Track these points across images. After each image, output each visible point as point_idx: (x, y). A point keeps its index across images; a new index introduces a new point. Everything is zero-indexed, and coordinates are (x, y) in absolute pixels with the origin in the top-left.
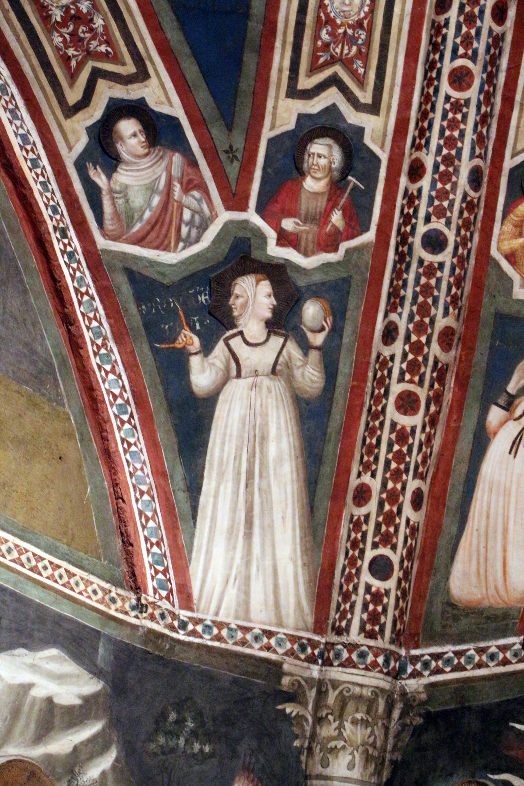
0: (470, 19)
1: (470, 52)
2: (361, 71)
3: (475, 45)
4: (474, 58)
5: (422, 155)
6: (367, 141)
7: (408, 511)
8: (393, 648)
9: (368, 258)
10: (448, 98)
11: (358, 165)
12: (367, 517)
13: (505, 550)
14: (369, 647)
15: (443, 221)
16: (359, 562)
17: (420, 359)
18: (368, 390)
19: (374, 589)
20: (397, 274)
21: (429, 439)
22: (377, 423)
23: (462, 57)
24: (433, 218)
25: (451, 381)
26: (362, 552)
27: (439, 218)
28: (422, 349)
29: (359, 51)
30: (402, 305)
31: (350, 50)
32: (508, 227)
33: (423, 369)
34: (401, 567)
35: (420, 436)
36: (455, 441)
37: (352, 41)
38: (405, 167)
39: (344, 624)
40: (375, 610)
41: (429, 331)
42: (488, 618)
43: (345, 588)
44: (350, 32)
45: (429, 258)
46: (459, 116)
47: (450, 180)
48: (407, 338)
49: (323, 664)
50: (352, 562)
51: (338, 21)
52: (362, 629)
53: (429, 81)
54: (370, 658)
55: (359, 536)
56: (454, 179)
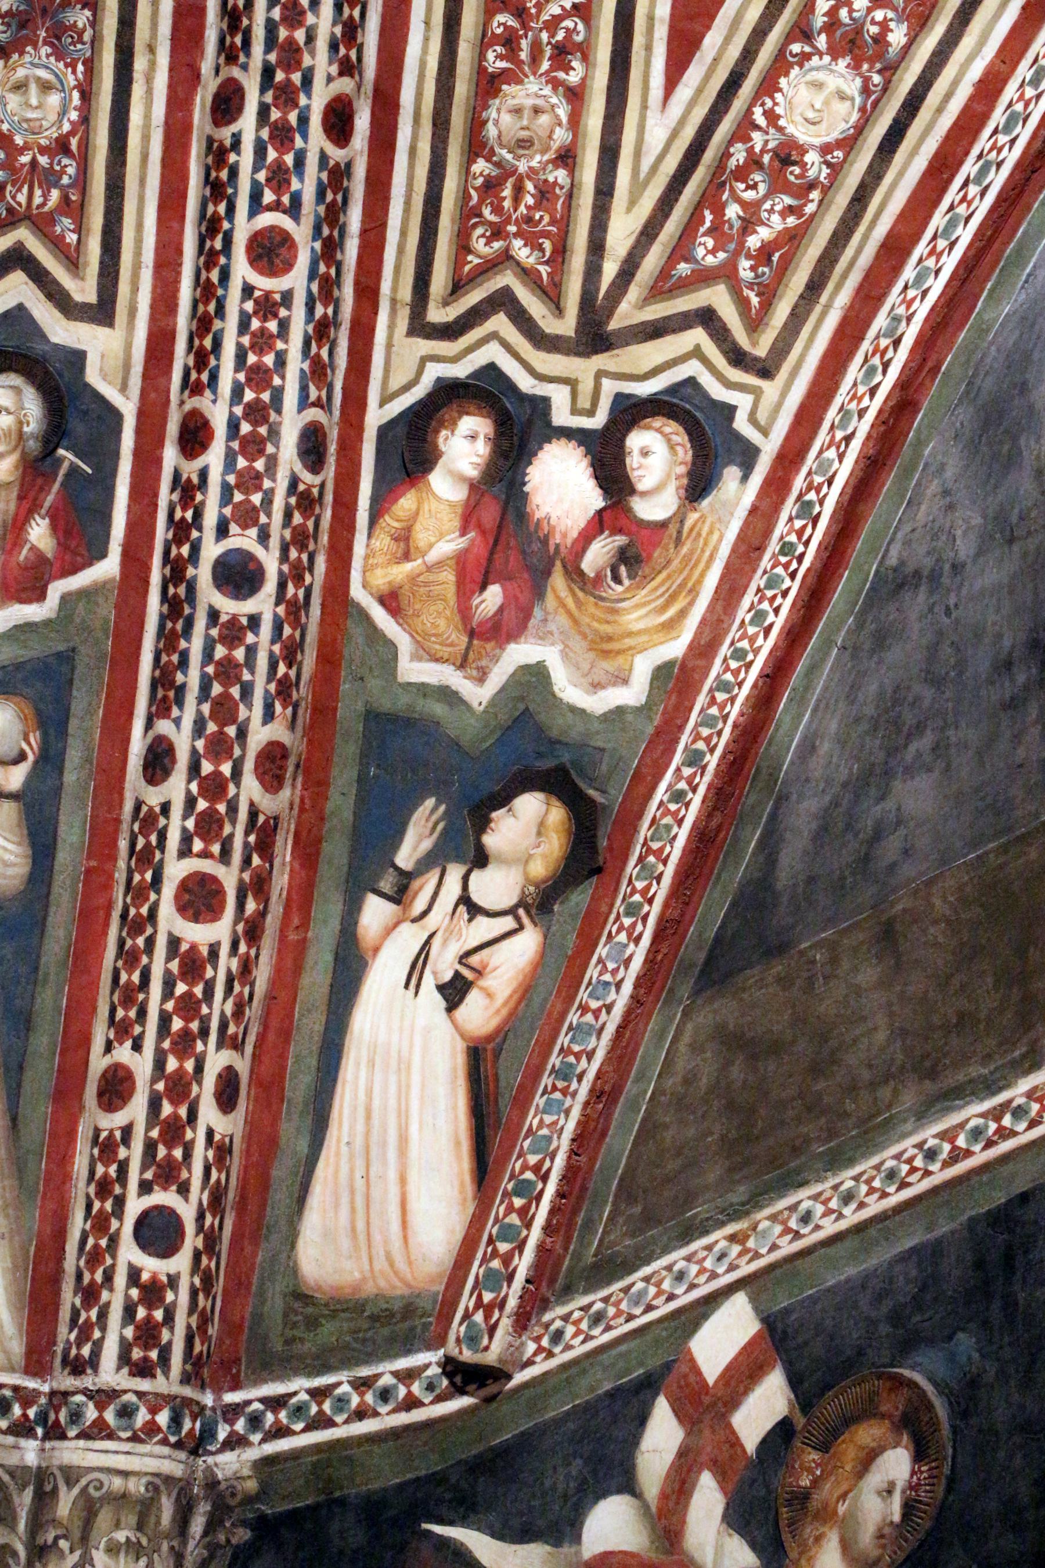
0: (282, 135)
1: (286, 199)
2: (72, 238)
3: (295, 185)
4: (294, 210)
5: (203, 403)
6: (93, 376)
7: (209, 1114)
8: (188, 1392)
9: (107, 611)
10: (248, 290)
11: (77, 426)
12: (127, 1131)
13: (403, 1180)
14: (140, 1394)
15: (253, 532)
16: (115, 1224)
17: (222, 808)
18: (120, 876)
19: (145, 1276)
20: (168, 640)
21: (247, 967)
22: (140, 941)
23: (269, 208)
24: (234, 528)
25: (284, 849)
26: (120, 1202)
27: (245, 527)
28: (224, 789)
29: (65, 199)
30: (180, 702)
31: (46, 196)
32: (382, 541)
33: (227, 830)
34: (200, 1228)
35: (227, 963)
36: (298, 969)
37: (50, 179)
38: (173, 428)
39: (86, 1351)
40: (149, 1318)
41: (237, 752)
42: (374, 1318)
43: (87, 1278)
44: (43, 160)
45: (228, 606)
46: (272, 326)
47: (261, 452)
48: (194, 768)
49: (46, 1437)
50: (100, 1224)
51: (19, 140)
52: (124, 1358)
53: (209, 258)
54: (142, 1416)
55: (113, 1170)
56: (270, 449)
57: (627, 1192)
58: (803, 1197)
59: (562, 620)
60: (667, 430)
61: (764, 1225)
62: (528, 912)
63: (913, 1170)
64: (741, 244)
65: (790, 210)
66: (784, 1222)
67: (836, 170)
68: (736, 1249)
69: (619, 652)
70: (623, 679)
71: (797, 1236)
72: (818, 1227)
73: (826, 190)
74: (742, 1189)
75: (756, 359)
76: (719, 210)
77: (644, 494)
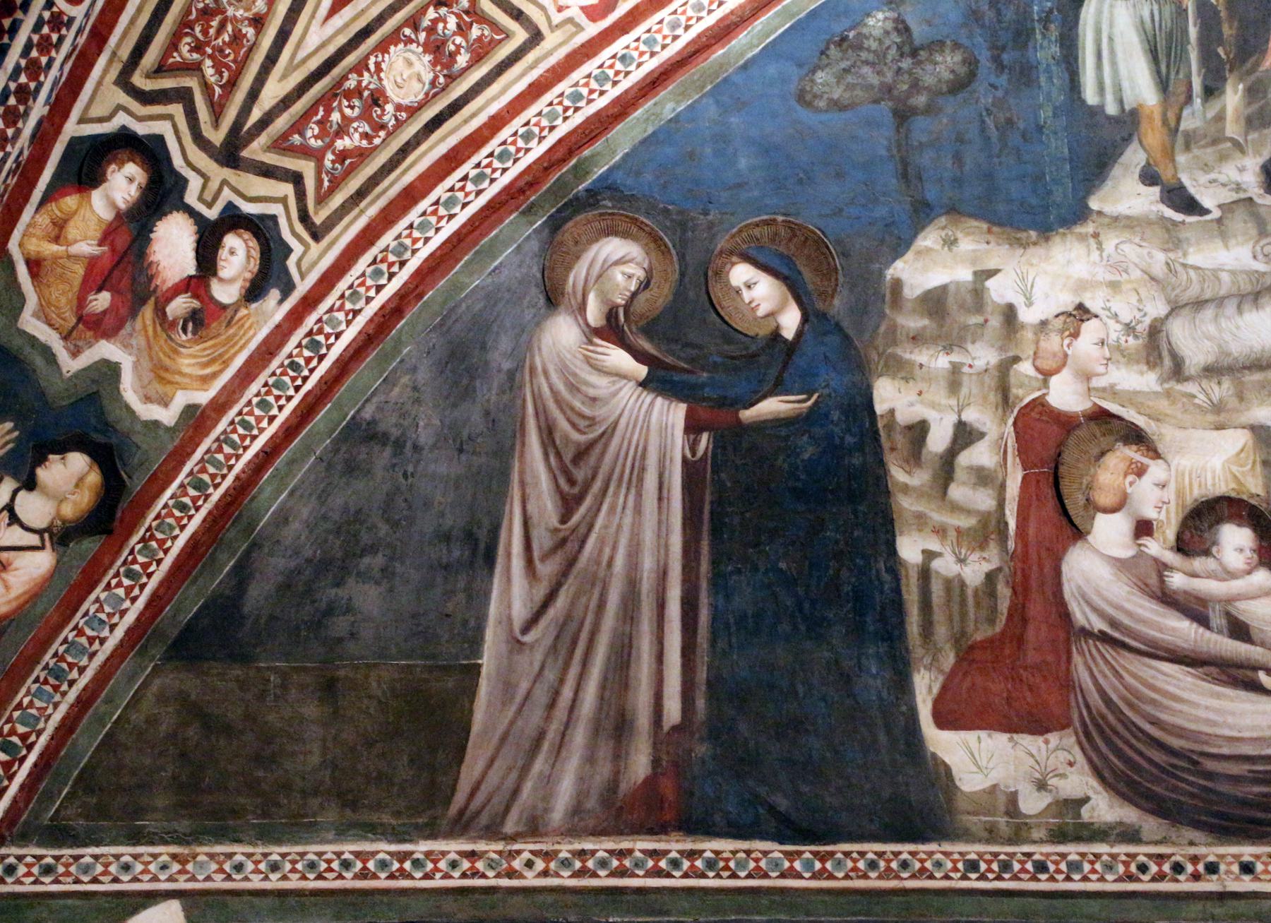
57: (86, 782)
58: (239, 851)
59: (143, 342)
60: (251, 244)
61: (201, 858)
62: (51, 538)
63: (330, 870)
64: (333, 142)
65: (365, 136)
66: (220, 863)
67: (399, 124)
68: (176, 867)
69: (170, 382)
70: (165, 402)
71: (229, 878)
72: (246, 879)
73: (389, 134)
74: (186, 823)
75: (313, 223)
76: (329, 111)
77: (221, 280)
